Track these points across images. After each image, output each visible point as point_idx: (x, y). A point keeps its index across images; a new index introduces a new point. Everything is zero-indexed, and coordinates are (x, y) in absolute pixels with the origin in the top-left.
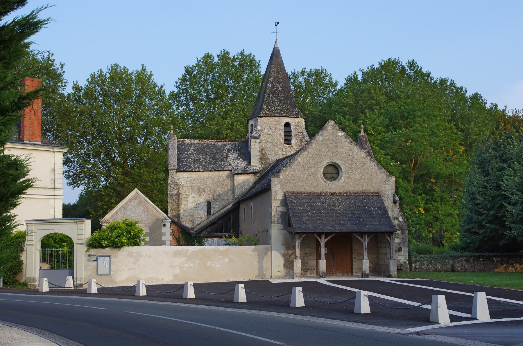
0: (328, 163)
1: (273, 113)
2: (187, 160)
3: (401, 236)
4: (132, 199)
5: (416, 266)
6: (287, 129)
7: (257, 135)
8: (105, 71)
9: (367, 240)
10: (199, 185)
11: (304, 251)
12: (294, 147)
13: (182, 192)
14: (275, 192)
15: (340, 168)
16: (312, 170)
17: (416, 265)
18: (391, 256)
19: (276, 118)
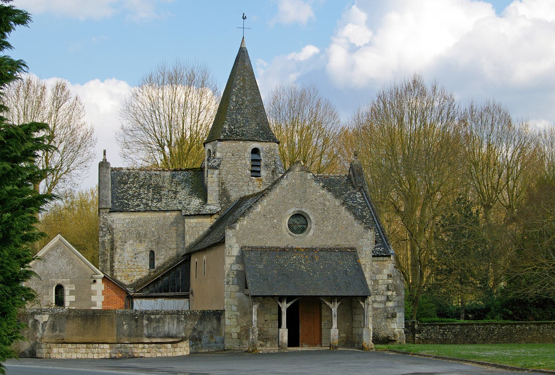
1: (237, 135)
2: (124, 195)
4: (54, 248)
7: (215, 164)
9: (337, 305)
10: (140, 229)
11: (264, 317)
12: (264, 180)
13: (116, 237)
14: (230, 246)
15: (309, 218)
16: (275, 221)
18: (364, 324)
19: (241, 142)
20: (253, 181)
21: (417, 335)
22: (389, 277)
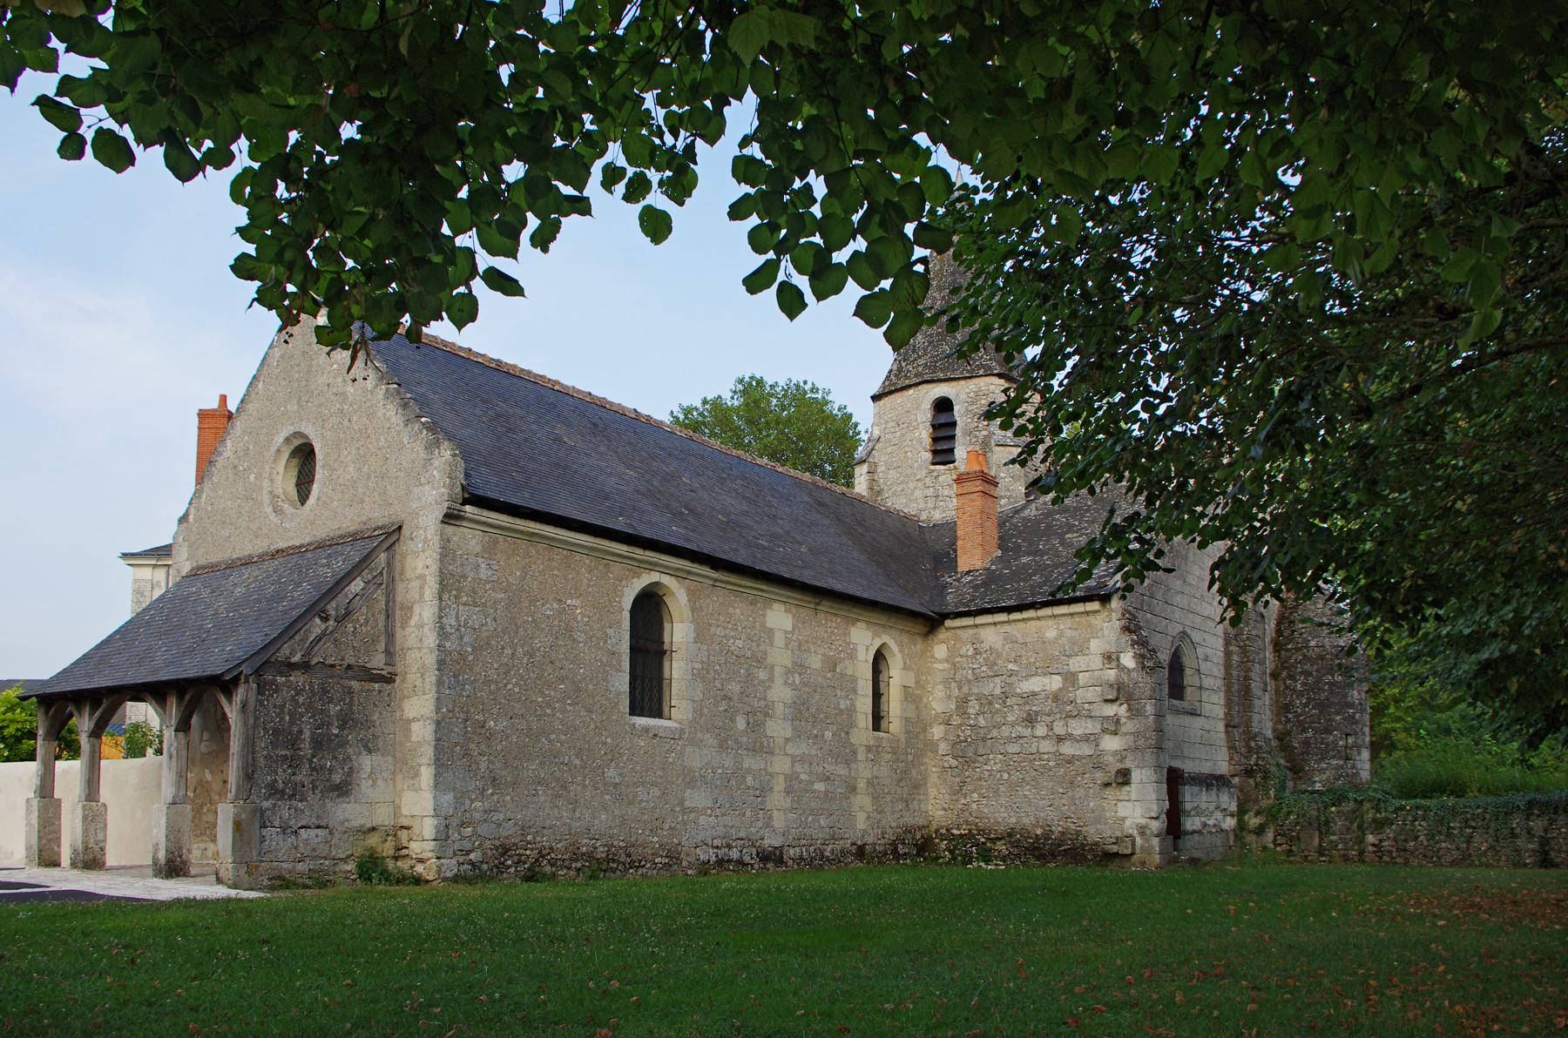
0: (287, 440)
5: (1381, 841)
6: (943, 419)
8: (782, 383)
17: (1380, 836)
19: (911, 391)
20: (935, 474)
21: (1370, 836)
22: (1106, 661)
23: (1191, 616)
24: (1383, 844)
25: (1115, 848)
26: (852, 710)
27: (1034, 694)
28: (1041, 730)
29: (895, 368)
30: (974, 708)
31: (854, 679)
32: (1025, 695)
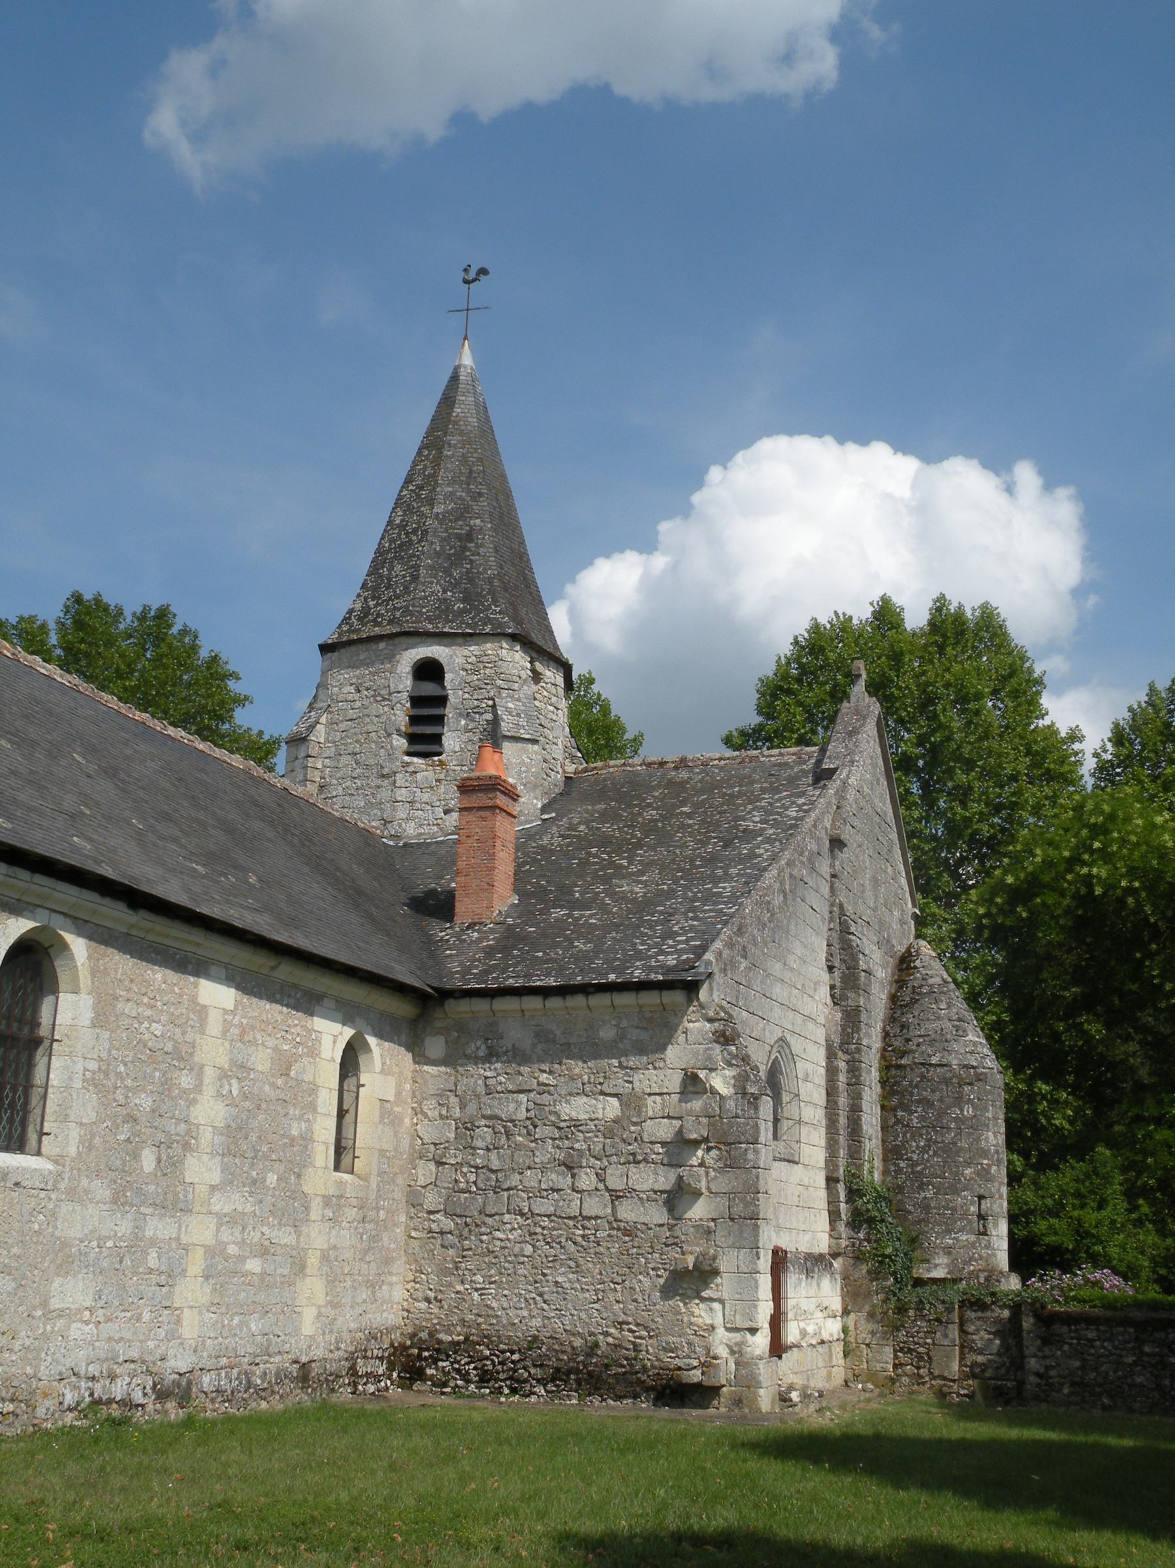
3: (722, 1183)
6: (429, 689)
12: (452, 765)
19: (382, 645)
20: (411, 769)
21: (1033, 1361)
23: (791, 1014)
24: (1052, 1373)
25: (696, 1376)
26: (306, 1139)
27: (576, 1124)
28: (587, 1180)
29: (358, 606)
30: (483, 1139)
31: (314, 1089)
32: (562, 1124)
